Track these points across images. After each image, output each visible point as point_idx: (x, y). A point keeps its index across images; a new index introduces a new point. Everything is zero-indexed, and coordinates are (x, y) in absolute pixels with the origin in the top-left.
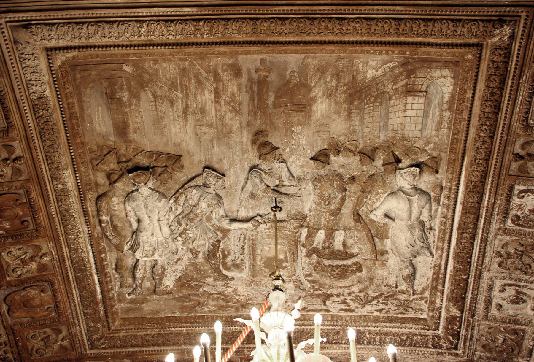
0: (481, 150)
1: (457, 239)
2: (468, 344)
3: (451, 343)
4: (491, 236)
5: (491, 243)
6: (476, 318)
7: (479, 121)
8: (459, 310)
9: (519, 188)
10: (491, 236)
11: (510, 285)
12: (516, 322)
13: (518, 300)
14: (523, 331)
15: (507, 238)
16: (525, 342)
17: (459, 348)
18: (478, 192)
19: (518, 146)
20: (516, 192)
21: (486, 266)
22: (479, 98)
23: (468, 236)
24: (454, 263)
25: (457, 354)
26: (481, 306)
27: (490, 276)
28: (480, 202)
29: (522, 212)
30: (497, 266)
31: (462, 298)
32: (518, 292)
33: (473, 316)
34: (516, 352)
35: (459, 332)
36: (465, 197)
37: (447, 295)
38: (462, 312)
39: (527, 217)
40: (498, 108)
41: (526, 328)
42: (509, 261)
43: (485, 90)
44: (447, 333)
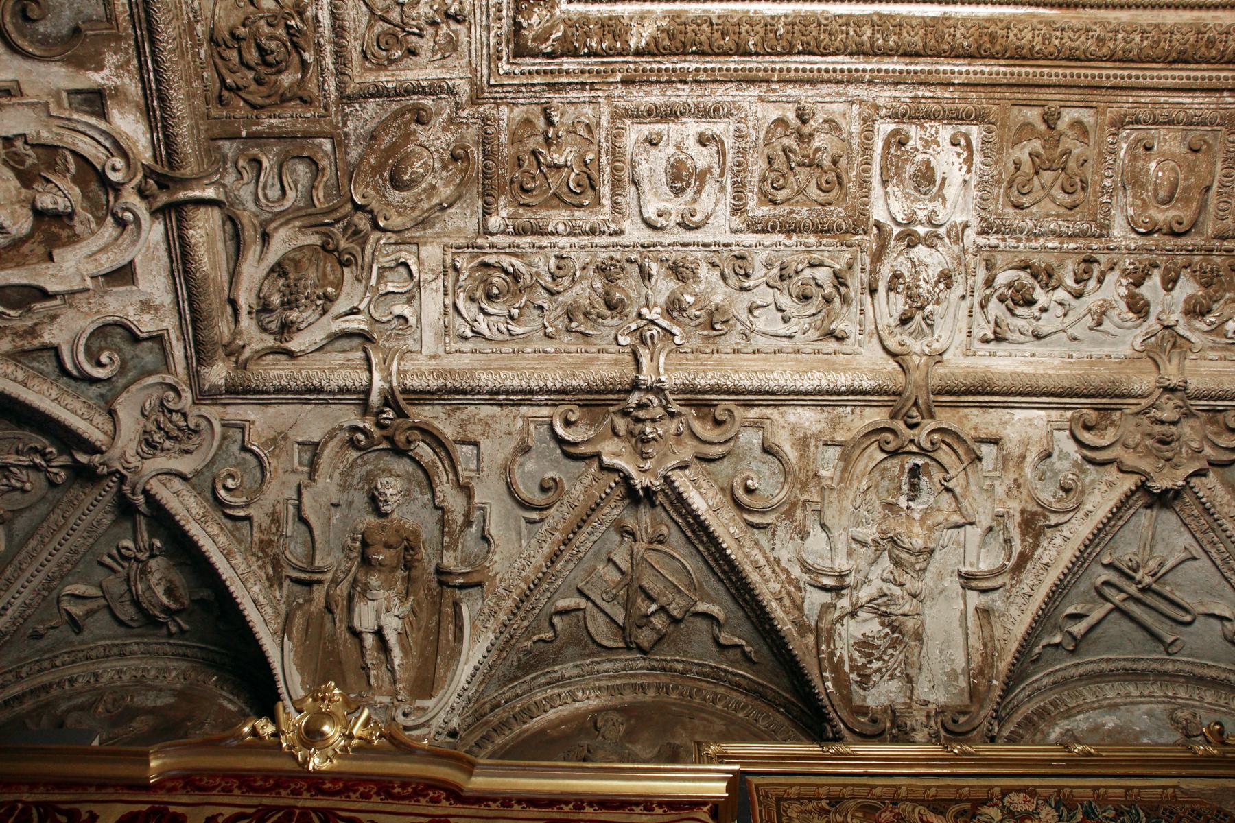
0: (1083, 38)
1: (851, 16)
2: (538, 80)
3: (542, 37)
4: (859, 92)
5: (839, 94)
6: (619, 90)
7: (1150, 25)
8: (647, 44)
9: (976, 133)
10: (859, 92)
11: (722, 155)
12: (616, 184)
13: (680, 177)
14: (599, 203)
15: (854, 127)
16: (565, 214)
17: (519, 60)
18: (978, 49)
19: (1076, 115)
20: (963, 129)
21: (774, 91)
22: (1199, 18)
23: (865, 38)
24: (786, 16)
25: (500, 59)
26: (655, 97)
27: (746, 105)
28: (956, 54)
29: (920, 148)
30: (774, 117)
31: (684, 45)
32: (701, 176)
33: (626, 82)
34: (527, 199)
35: (575, 54)
36: (965, 19)
37: (686, 11)
38: (638, 53)
39: (907, 160)
40: (1182, 59)
41: (607, 209)
42: (790, 142)
43: (1221, 25)
44: (569, 23)
